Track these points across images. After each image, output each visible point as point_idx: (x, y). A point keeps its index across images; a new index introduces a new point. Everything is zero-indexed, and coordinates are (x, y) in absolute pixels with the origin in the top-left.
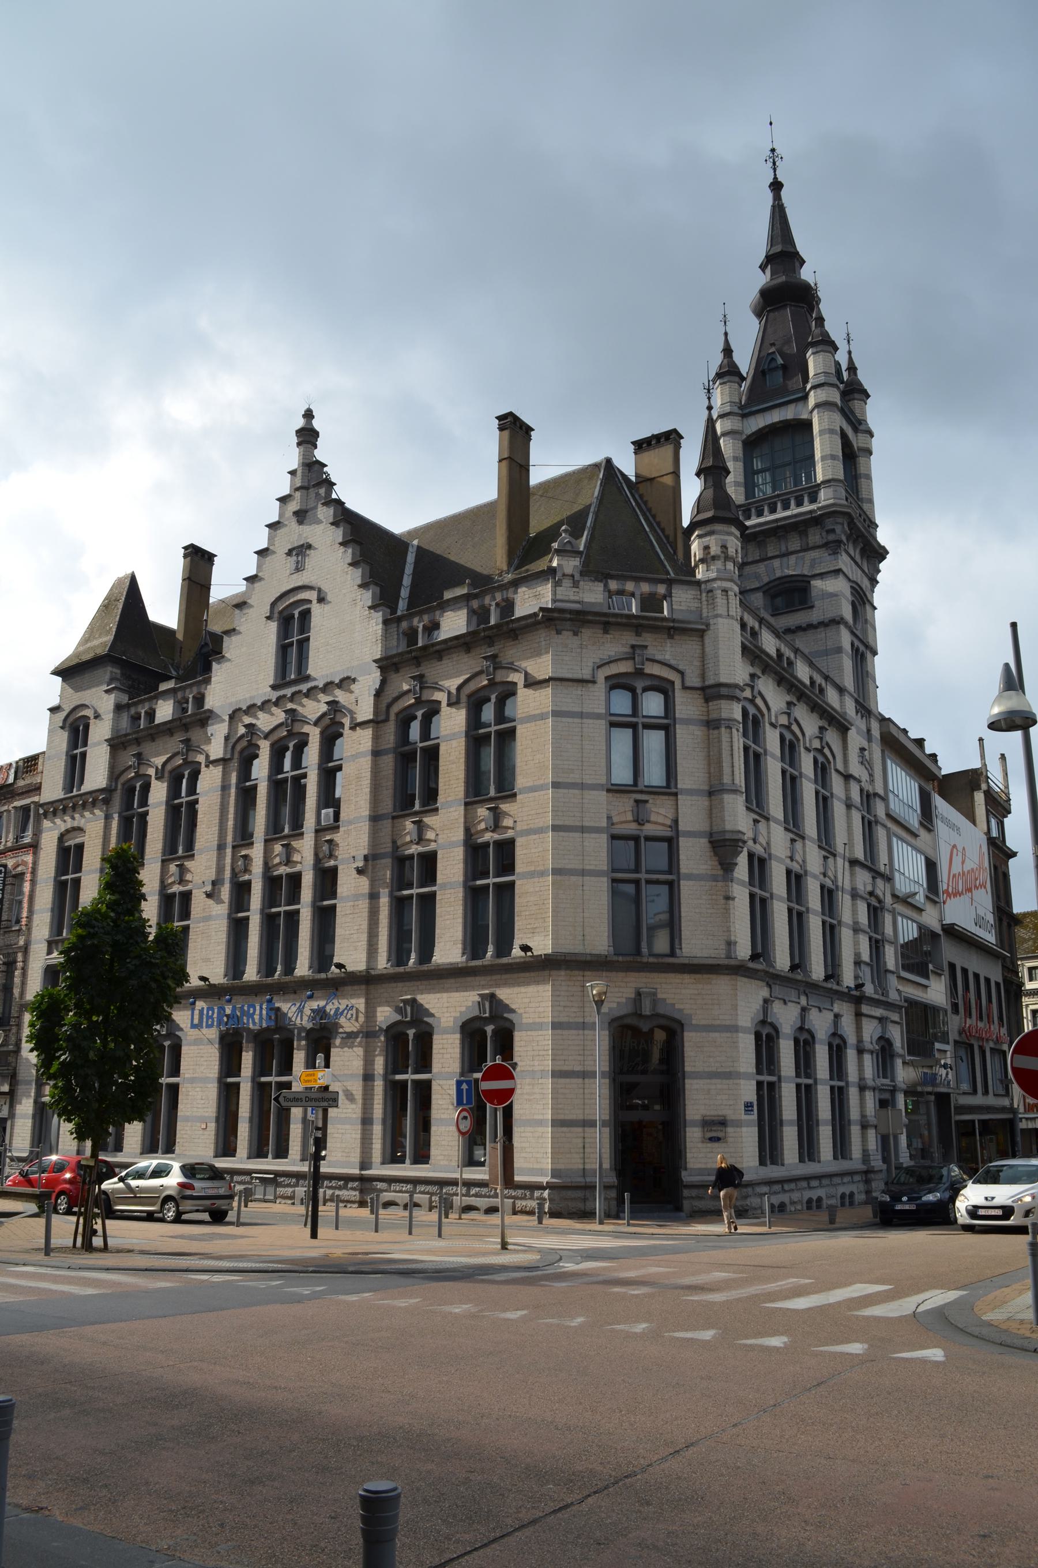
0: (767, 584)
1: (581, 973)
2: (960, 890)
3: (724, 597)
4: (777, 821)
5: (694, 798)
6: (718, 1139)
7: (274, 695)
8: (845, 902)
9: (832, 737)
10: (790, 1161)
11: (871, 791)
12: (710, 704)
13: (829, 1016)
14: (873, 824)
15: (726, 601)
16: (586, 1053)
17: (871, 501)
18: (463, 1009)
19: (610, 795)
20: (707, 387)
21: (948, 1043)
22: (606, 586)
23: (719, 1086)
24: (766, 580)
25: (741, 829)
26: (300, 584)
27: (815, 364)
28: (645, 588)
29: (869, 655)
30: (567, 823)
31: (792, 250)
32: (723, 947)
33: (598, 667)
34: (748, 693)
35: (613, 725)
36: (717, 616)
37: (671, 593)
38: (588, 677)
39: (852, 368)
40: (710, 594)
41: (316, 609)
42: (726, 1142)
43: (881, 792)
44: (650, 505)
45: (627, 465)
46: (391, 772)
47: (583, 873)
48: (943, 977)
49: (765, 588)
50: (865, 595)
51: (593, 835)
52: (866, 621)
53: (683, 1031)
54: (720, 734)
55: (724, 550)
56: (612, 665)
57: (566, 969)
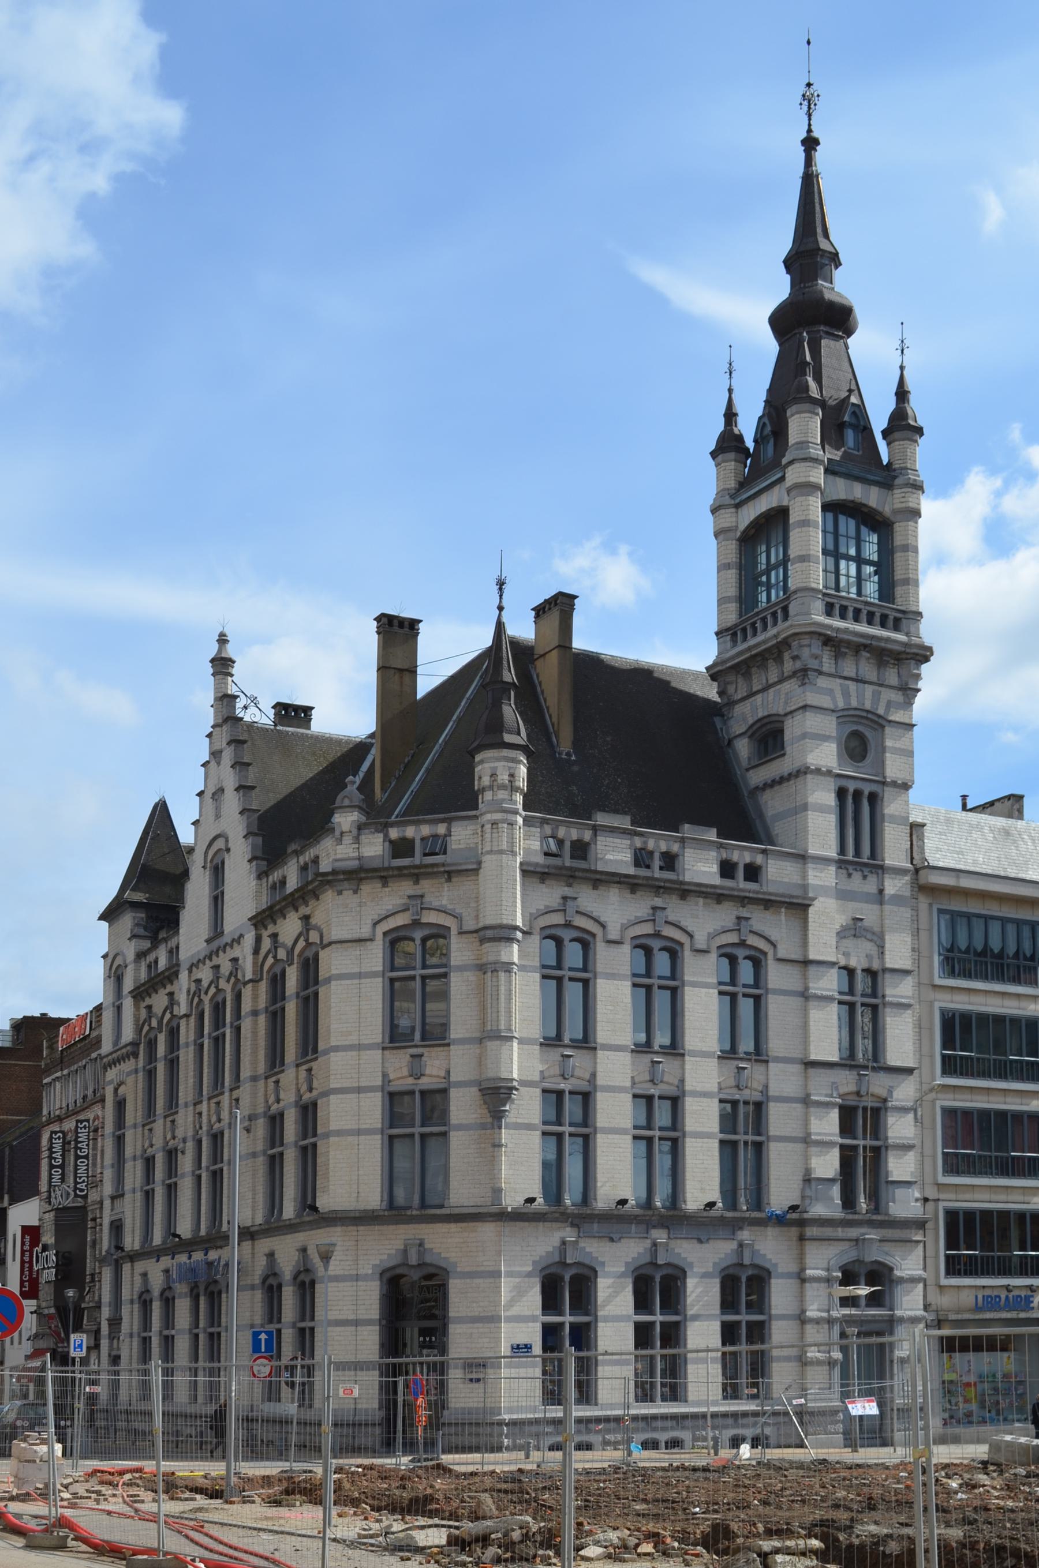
1: (355, 1228)
5: (467, 1046)
6: (478, 1380)
16: (359, 1302)
19: (387, 1052)
22: (386, 836)
23: (481, 1330)
30: (345, 1085)
33: (376, 924)
44: (543, 687)
47: (359, 1132)
49: (749, 733)
56: (389, 919)
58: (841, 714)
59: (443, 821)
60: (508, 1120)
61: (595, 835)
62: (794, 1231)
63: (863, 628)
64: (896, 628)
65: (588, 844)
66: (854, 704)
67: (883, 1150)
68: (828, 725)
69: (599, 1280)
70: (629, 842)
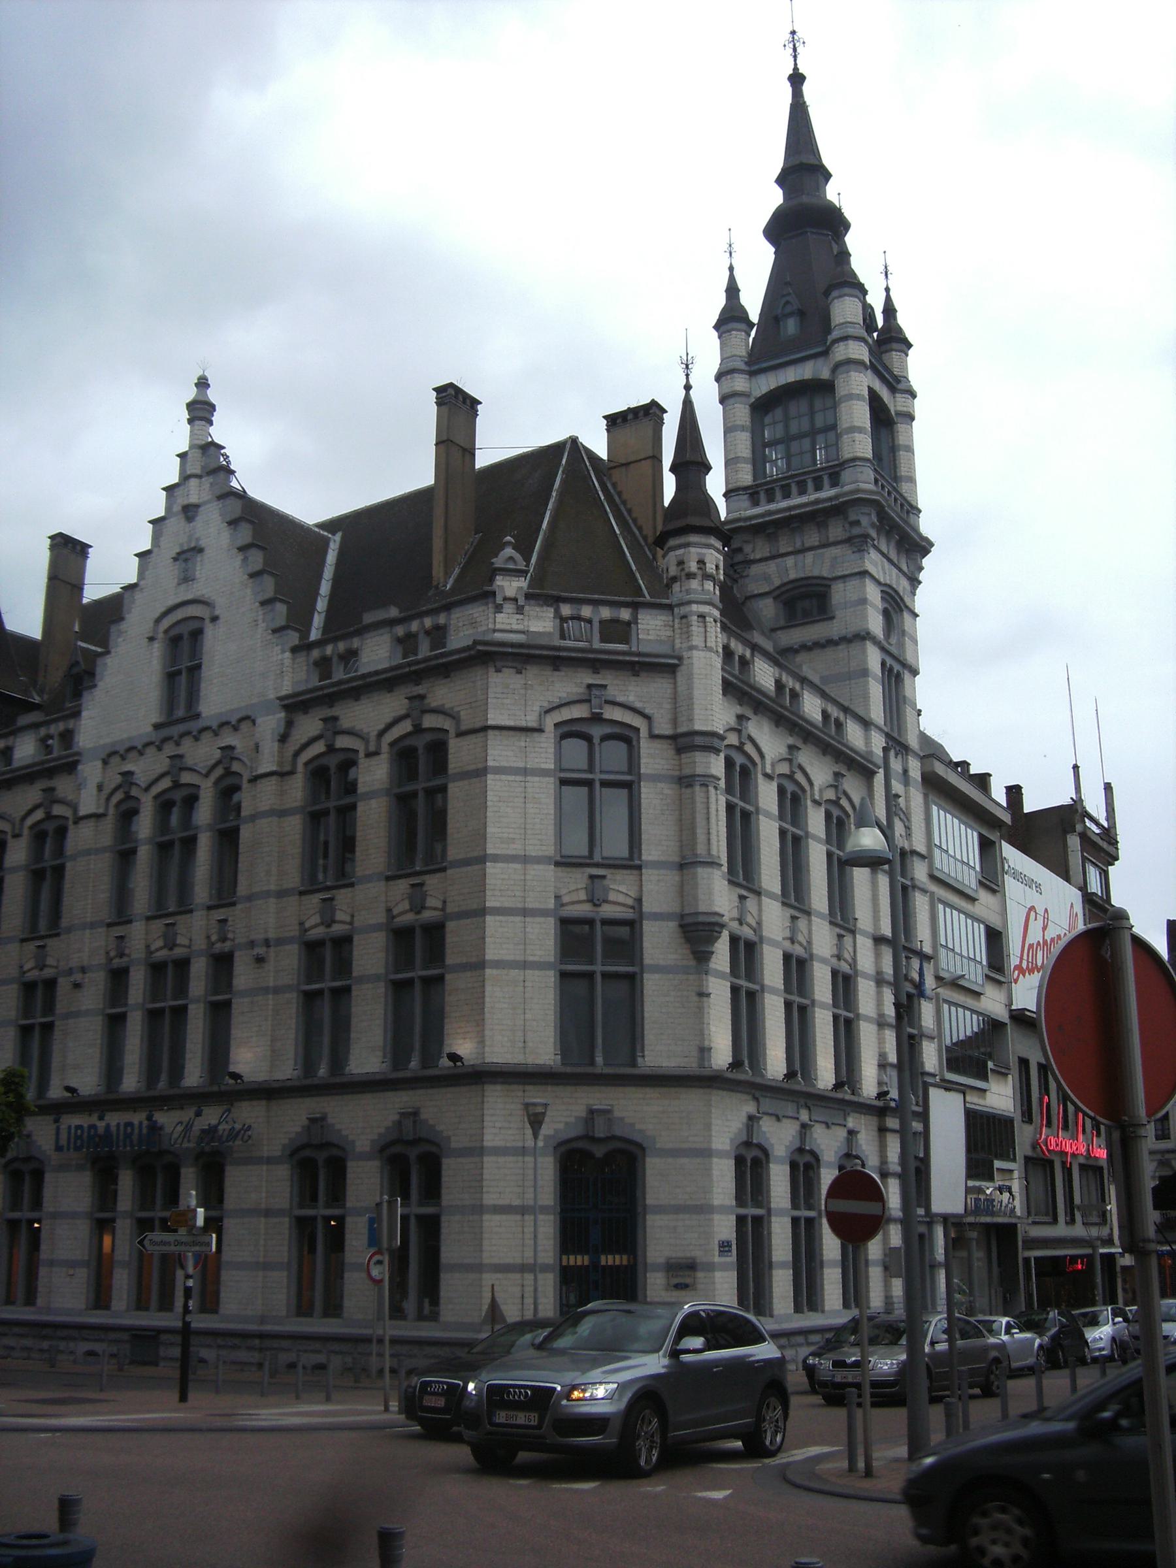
0: (778, 588)
1: (521, 1087)
2: (1039, 964)
3: (701, 624)
4: (771, 896)
5: (662, 872)
7: (156, 737)
8: (866, 992)
9: (853, 786)
10: (782, 1312)
11: (907, 847)
12: (683, 756)
13: (842, 1133)
14: (910, 889)
15: (702, 630)
17: (912, 480)
18: (382, 1130)
20: (685, 362)
21: (1014, 1160)
22: (557, 612)
24: (777, 583)
25: (717, 909)
26: (190, 597)
27: (845, 311)
28: (606, 613)
29: (907, 676)
30: (506, 905)
31: (814, 162)
32: (695, 1053)
34: (733, 739)
35: (564, 782)
36: (691, 648)
37: (637, 619)
39: (890, 310)
40: (684, 621)
41: (209, 631)
42: (695, 1289)
43: (921, 848)
44: (625, 497)
45: (598, 443)
46: (297, 836)
47: (524, 965)
48: (1010, 1076)
50: (902, 599)
52: (903, 633)
53: (644, 1156)
54: (693, 793)
55: (702, 566)
57: (503, 1083)
59: (626, 605)
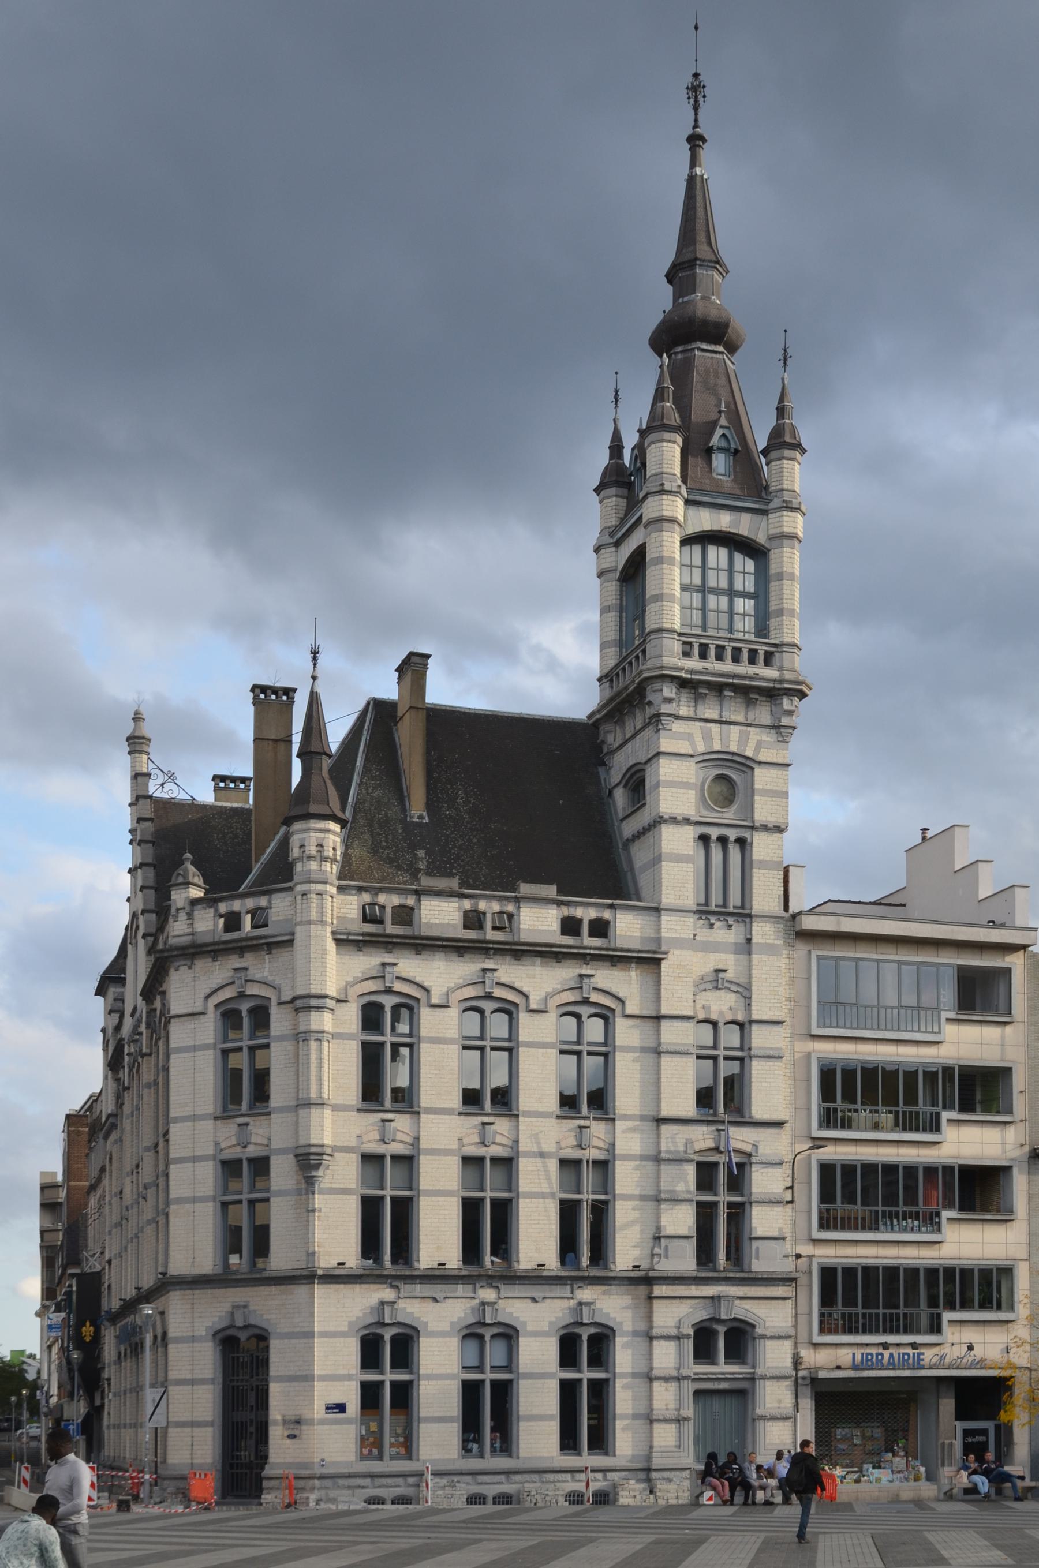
5: (284, 1115)
19: (219, 1122)
22: (216, 910)
30: (183, 1155)
33: (208, 997)
38: (199, 1009)
40: (305, 897)
42: (301, 1439)
51: (203, 1164)
56: (220, 993)
58: (701, 758)
60: (322, 1185)
61: (419, 900)
62: (642, 1290)
63: (727, 666)
64: (768, 661)
65: (412, 909)
66: (717, 747)
67: (747, 1206)
68: (688, 772)
69: (421, 1339)
70: (457, 905)
